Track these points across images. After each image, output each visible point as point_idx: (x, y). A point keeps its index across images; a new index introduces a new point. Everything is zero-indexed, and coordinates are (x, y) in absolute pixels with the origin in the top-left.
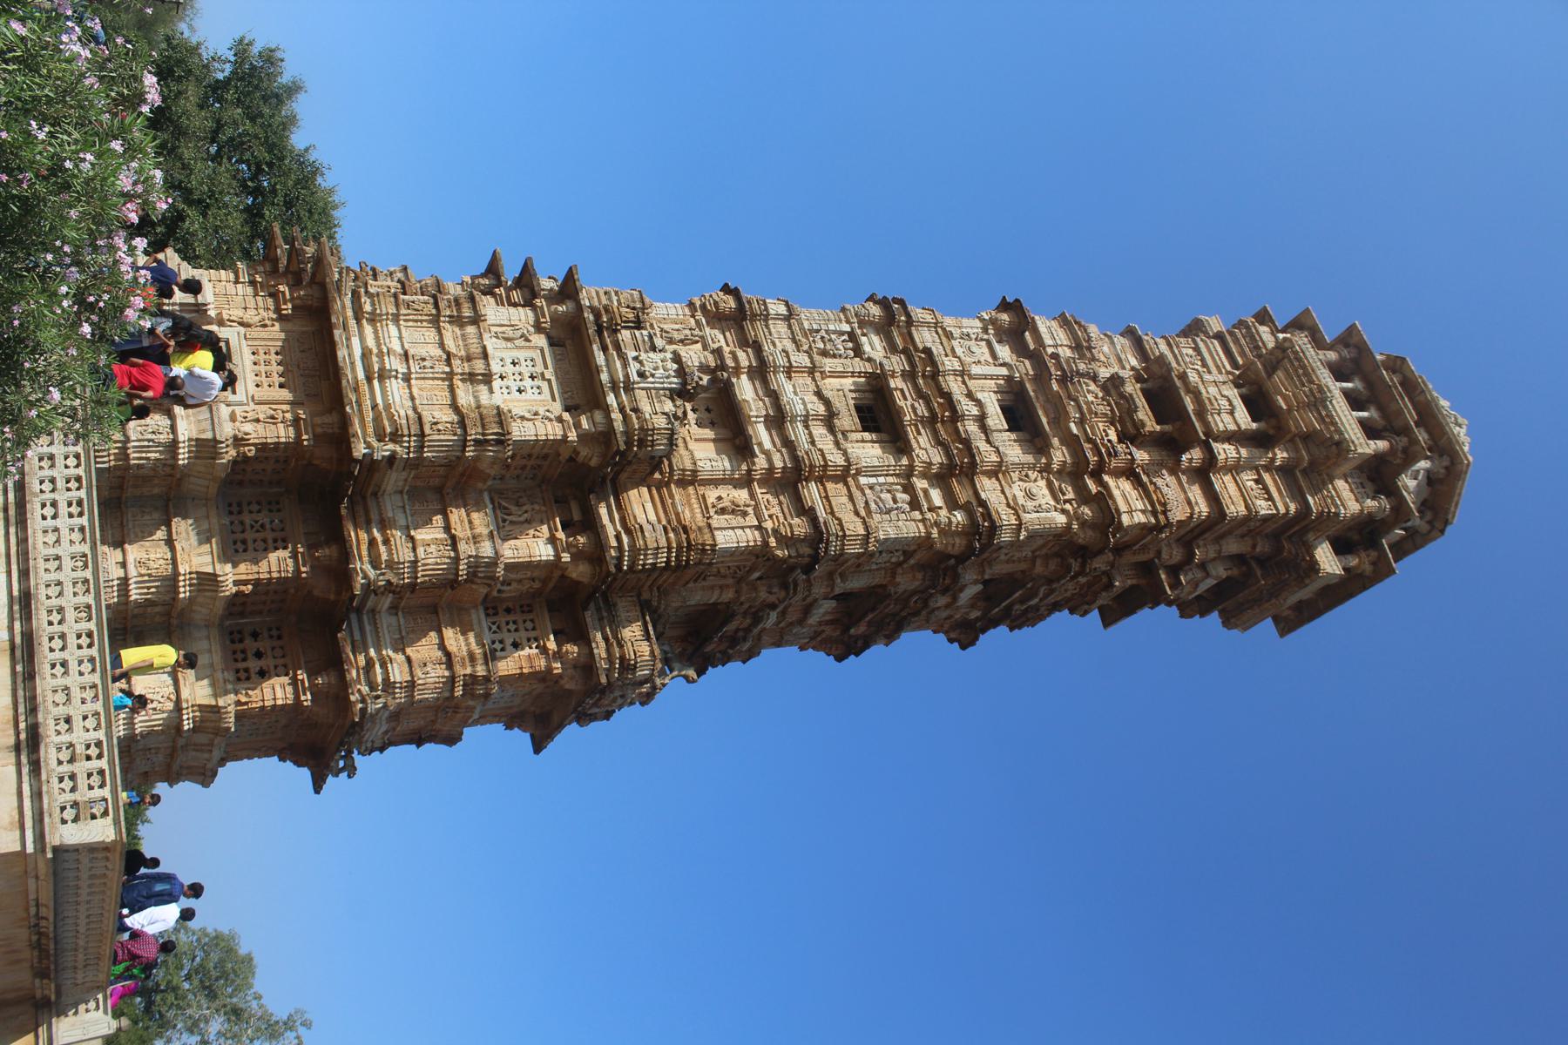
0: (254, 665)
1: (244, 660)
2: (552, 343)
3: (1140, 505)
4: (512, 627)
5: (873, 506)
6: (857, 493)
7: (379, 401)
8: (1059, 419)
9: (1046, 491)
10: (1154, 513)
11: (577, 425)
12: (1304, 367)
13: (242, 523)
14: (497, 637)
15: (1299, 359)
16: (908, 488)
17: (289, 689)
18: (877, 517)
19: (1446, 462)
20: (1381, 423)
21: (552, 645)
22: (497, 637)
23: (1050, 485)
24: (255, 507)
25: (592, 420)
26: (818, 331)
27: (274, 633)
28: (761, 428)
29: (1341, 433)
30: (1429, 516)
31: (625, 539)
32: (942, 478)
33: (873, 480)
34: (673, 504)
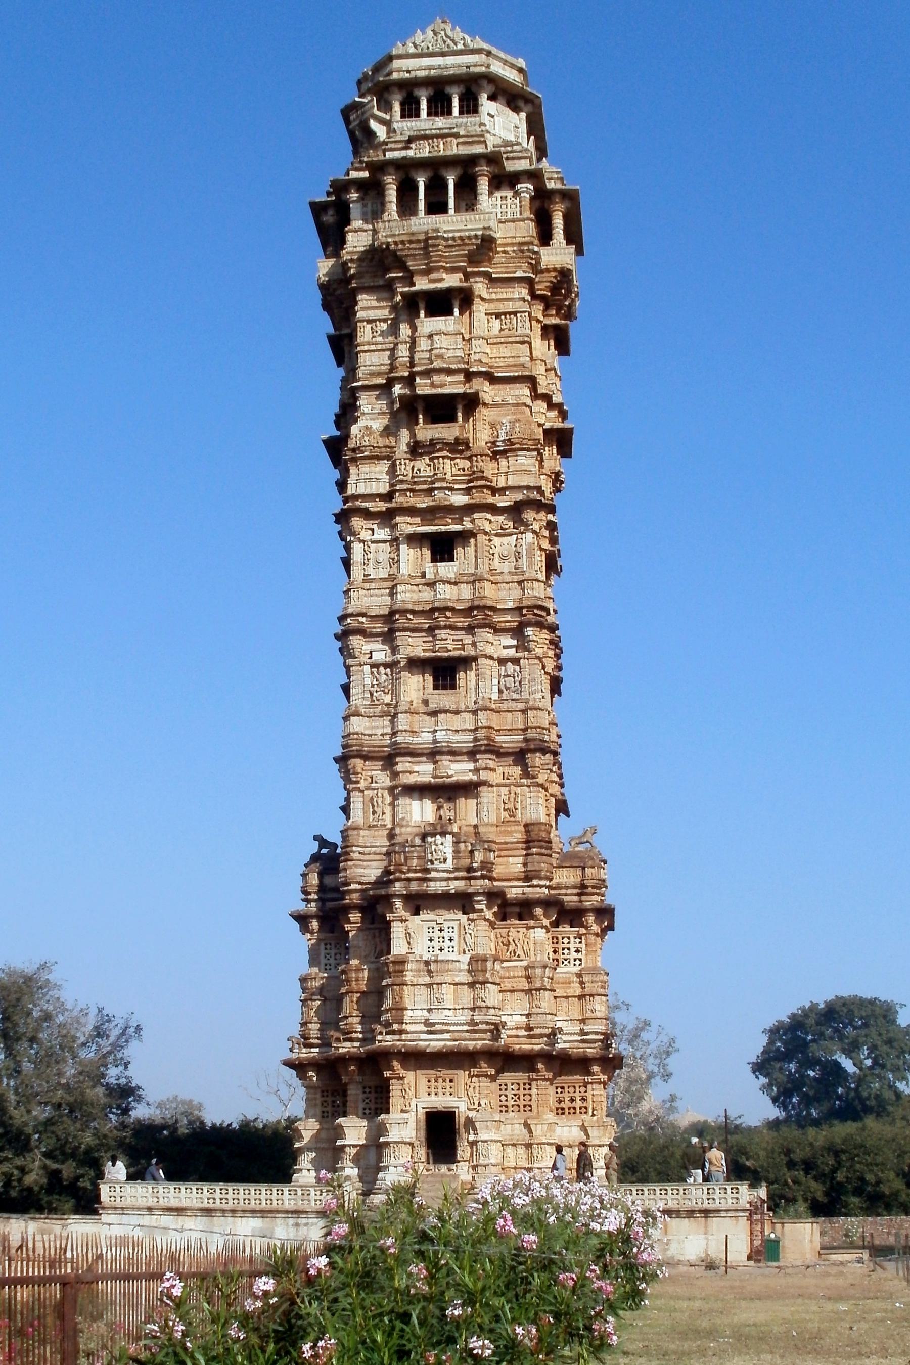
0: (578, 1104)
1: (574, 1108)
2: (417, 913)
3: (522, 460)
4: (566, 951)
5: (515, 696)
6: (504, 706)
7: (466, 1028)
8: (450, 509)
9: (506, 540)
10: (528, 450)
11: (482, 911)
12: (411, 242)
13: (513, 1106)
14: (572, 962)
15: (403, 242)
16: (502, 662)
17: (594, 1086)
18: (525, 695)
19: (484, 83)
20: (459, 171)
21: (583, 931)
22: (572, 962)
23: (497, 535)
24: (503, 1098)
25: (478, 902)
26: (372, 694)
27: (559, 1090)
28: (456, 767)
29: (476, 236)
30: (521, 104)
31: (535, 882)
32: (497, 631)
33: (496, 689)
34: (512, 843)
